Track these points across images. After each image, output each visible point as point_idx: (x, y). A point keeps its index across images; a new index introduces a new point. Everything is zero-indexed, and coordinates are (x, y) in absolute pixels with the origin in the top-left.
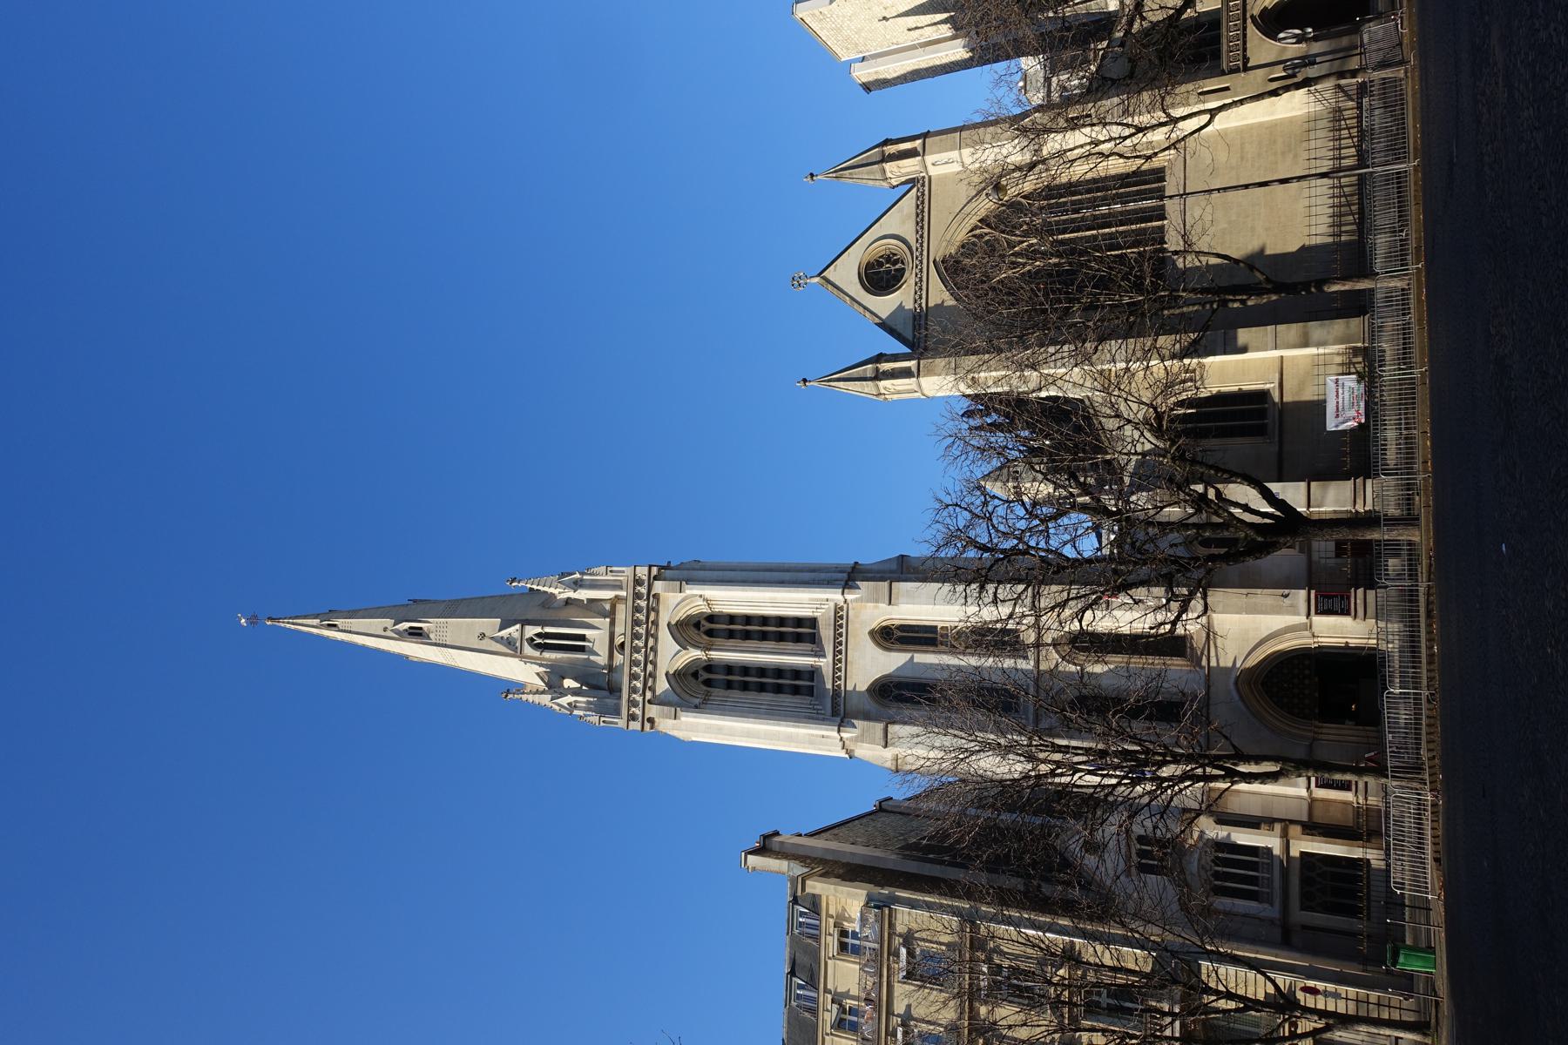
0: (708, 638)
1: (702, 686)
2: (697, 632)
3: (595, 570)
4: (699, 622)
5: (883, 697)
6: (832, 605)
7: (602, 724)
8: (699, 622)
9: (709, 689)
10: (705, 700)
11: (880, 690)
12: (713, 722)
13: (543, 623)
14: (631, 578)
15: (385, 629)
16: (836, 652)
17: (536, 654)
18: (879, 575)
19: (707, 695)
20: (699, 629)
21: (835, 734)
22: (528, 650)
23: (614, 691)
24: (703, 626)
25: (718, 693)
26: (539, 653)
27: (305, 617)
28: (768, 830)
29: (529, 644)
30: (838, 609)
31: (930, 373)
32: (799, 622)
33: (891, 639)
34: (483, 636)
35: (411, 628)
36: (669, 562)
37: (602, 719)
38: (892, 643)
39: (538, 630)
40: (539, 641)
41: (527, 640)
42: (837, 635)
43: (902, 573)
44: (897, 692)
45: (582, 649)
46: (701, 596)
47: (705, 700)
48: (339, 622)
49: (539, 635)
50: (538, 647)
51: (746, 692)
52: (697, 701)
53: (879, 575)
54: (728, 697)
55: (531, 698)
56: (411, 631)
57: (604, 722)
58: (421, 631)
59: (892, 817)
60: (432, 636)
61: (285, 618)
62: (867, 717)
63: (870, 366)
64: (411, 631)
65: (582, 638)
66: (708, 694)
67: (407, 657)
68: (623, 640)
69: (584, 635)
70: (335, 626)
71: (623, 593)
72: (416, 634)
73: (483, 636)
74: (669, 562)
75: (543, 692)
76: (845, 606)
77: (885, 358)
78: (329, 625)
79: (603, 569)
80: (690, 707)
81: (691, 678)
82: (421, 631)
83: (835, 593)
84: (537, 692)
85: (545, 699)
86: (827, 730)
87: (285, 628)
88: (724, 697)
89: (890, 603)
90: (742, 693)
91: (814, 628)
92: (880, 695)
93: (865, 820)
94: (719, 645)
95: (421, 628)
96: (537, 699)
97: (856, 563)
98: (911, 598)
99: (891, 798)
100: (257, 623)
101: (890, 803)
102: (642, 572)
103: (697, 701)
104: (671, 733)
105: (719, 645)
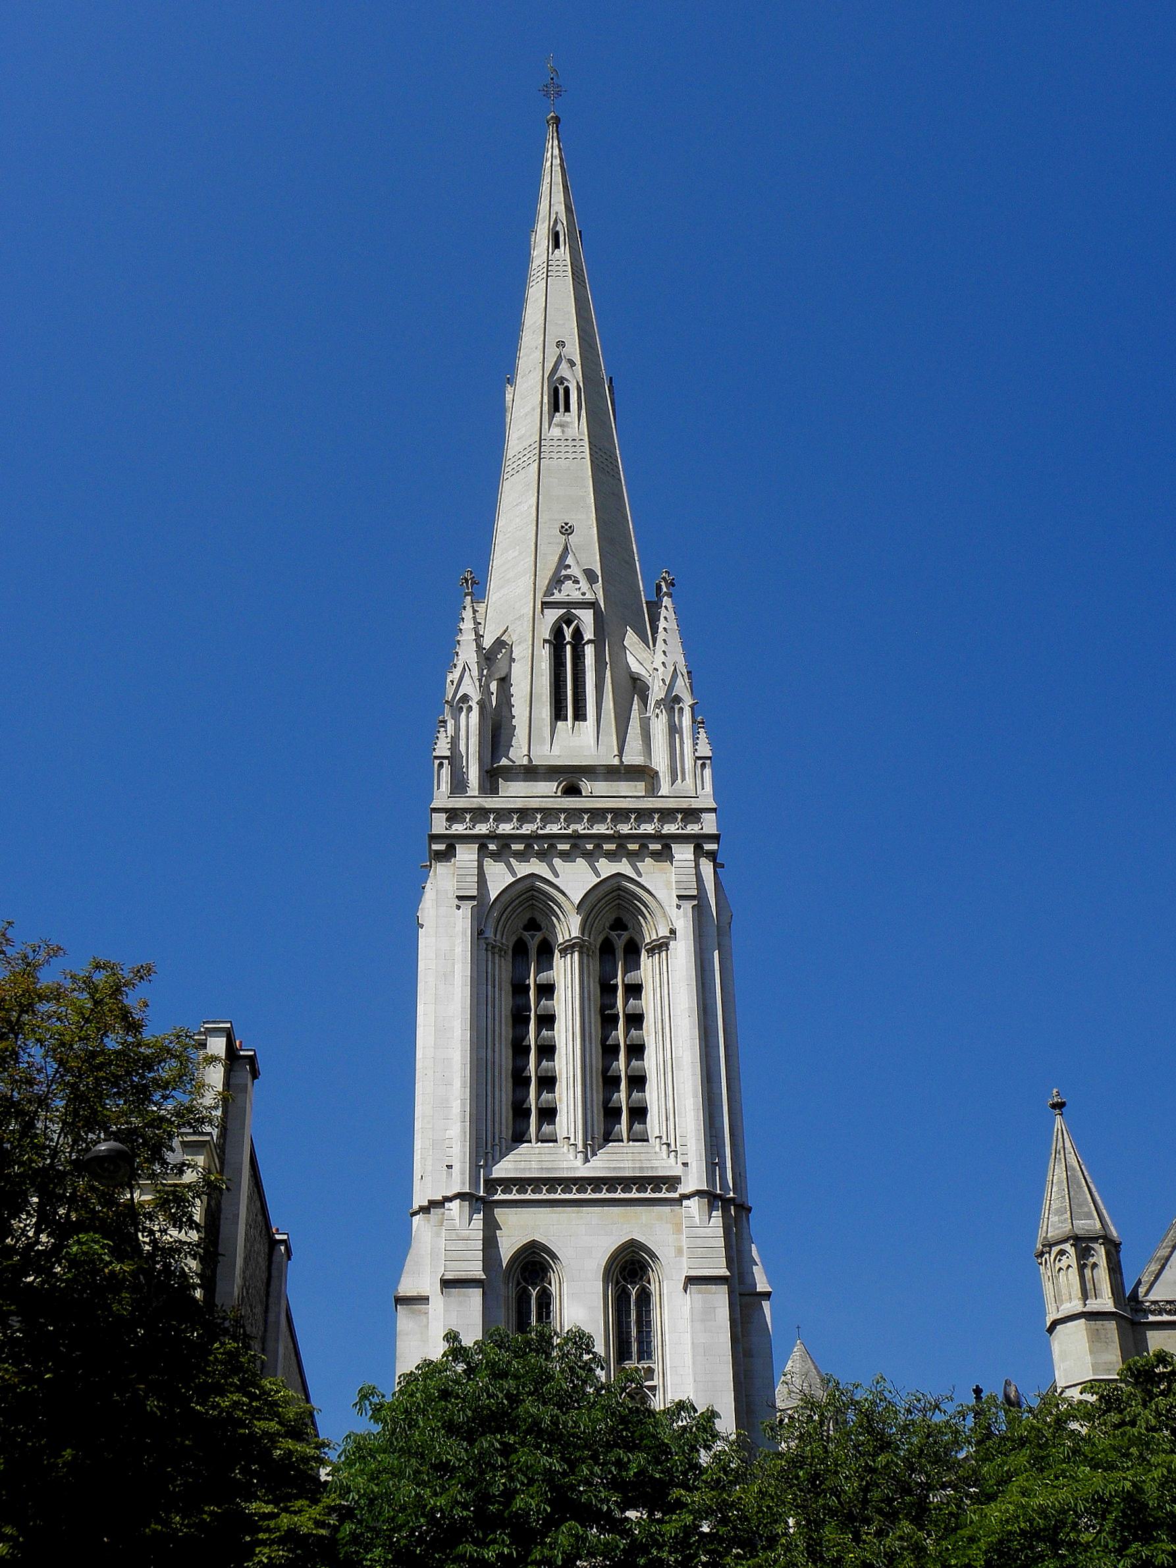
0: (598, 947)
1: (514, 938)
2: (608, 925)
3: (702, 735)
4: (624, 928)
5: (524, 1269)
6: (677, 1171)
7: (437, 762)
8: (624, 928)
9: (510, 952)
10: (493, 947)
11: (534, 1263)
12: (458, 967)
13: (598, 642)
14: (695, 804)
15: (560, 344)
16: (597, 1183)
17: (546, 633)
18: (735, 1255)
19: (500, 950)
20: (612, 928)
21: (458, 1182)
22: (553, 615)
23: (491, 777)
24: (619, 936)
25: (504, 970)
26: (547, 637)
27: (565, 187)
28: (261, 1065)
29: (561, 618)
30: (672, 1182)
31: (1095, 1338)
32: (639, 1113)
33: (625, 1279)
34: (567, 530)
35: (567, 390)
36: (722, 866)
37: (446, 762)
38: (618, 1283)
39: (588, 635)
40: (568, 633)
41: (568, 613)
42: (627, 1183)
43: (740, 1295)
44: (534, 1293)
45: (558, 714)
46: (673, 932)
47: (493, 947)
48: (563, 253)
49: (578, 634)
50: (558, 633)
51: (510, 1019)
52: (490, 933)
53: (735, 1255)
54: (500, 990)
55: (467, 625)
56: (561, 392)
57: (441, 765)
58: (562, 409)
59: (263, 1264)
60: (556, 432)
61: (560, 149)
62: (490, 1243)
63: (1098, 1225)
64: (561, 392)
65: (580, 715)
66: (502, 951)
67: (511, 381)
68: (584, 794)
69: (585, 719)
70: (557, 246)
71: (665, 789)
72: (557, 400)
73: (567, 530)
74: (722, 866)
75: (479, 647)
76: (676, 1195)
77: (1114, 1252)
78: (556, 235)
79: (705, 750)
80: (479, 924)
81: (528, 916)
82: (562, 409)
83: (699, 1179)
84: (479, 637)
85: (467, 654)
86: (463, 1174)
87: (543, 149)
88: (500, 984)
89: (691, 1280)
90: (509, 1013)
91: (629, 1140)
92: (528, 1263)
93: (260, 1218)
94: (588, 967)
95: (567, 409)
96: (467, 637)
97: (749, 1210)
98: (704, 1316)
99: (289, 1259)
100: (547, 95)
101: (285, 1257)
102: (709, 824)
103: (490, 933)
104: (428, 886)
105: (588, 967)
